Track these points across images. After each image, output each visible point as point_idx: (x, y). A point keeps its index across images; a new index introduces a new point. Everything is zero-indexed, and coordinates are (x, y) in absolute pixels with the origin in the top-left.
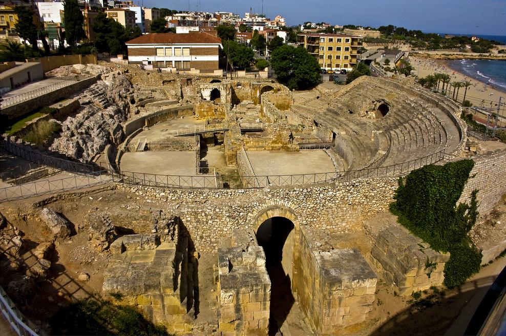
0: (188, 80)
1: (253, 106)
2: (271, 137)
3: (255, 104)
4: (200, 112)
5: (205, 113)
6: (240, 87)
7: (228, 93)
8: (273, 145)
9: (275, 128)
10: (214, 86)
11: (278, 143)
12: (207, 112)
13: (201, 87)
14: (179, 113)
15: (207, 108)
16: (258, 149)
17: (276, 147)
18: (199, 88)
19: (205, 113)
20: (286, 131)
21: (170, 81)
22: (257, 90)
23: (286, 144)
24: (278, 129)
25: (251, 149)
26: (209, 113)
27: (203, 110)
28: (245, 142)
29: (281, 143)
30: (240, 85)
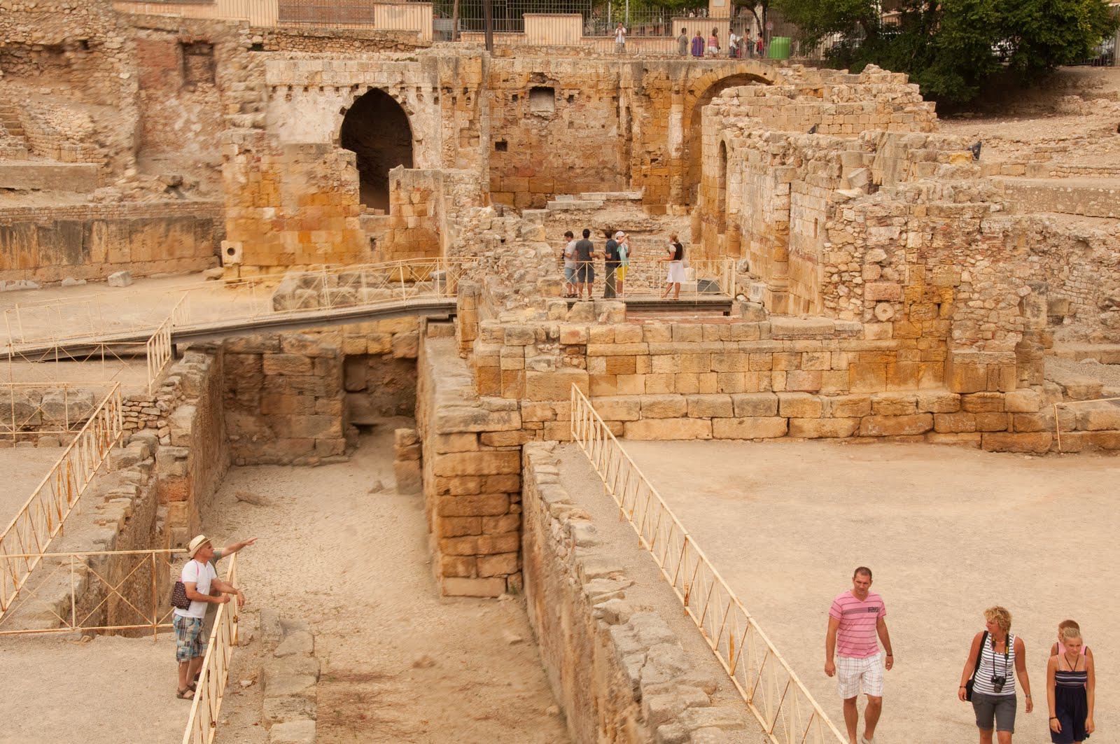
0: (187, 47)
1: (641, 215)
2: (848, 319)
3: (654, 204)
4: (255, 232)
5: (290, 240)
6: (545, 106)
7: (462, 120)
8: (860, 391)
9: (879, 234)
10: (364, 68)
11: (913, 375)
12: (305, 228)
13: (271, 78)
14: (98, 248)
15: (303, 201)
16: (723, 427)
17: (897, 410)
18: (254, 81)
19: (290, 240)
20: (994, 255)
21: (56, 50)
22: (668, 106)
23: (995, 377)
24: (913, 240)
25: (659, 427)
26: (321, 239)
27: (269, 213)
28: (599, 366)
29: (944, 376)
30: (550, 91)
